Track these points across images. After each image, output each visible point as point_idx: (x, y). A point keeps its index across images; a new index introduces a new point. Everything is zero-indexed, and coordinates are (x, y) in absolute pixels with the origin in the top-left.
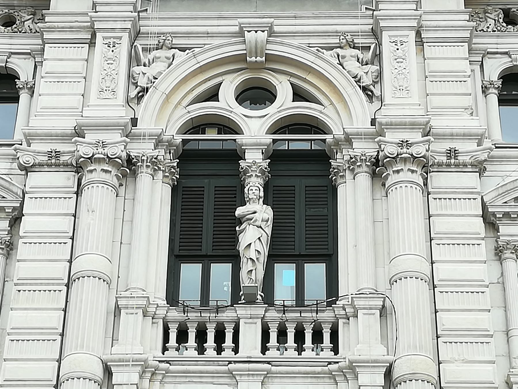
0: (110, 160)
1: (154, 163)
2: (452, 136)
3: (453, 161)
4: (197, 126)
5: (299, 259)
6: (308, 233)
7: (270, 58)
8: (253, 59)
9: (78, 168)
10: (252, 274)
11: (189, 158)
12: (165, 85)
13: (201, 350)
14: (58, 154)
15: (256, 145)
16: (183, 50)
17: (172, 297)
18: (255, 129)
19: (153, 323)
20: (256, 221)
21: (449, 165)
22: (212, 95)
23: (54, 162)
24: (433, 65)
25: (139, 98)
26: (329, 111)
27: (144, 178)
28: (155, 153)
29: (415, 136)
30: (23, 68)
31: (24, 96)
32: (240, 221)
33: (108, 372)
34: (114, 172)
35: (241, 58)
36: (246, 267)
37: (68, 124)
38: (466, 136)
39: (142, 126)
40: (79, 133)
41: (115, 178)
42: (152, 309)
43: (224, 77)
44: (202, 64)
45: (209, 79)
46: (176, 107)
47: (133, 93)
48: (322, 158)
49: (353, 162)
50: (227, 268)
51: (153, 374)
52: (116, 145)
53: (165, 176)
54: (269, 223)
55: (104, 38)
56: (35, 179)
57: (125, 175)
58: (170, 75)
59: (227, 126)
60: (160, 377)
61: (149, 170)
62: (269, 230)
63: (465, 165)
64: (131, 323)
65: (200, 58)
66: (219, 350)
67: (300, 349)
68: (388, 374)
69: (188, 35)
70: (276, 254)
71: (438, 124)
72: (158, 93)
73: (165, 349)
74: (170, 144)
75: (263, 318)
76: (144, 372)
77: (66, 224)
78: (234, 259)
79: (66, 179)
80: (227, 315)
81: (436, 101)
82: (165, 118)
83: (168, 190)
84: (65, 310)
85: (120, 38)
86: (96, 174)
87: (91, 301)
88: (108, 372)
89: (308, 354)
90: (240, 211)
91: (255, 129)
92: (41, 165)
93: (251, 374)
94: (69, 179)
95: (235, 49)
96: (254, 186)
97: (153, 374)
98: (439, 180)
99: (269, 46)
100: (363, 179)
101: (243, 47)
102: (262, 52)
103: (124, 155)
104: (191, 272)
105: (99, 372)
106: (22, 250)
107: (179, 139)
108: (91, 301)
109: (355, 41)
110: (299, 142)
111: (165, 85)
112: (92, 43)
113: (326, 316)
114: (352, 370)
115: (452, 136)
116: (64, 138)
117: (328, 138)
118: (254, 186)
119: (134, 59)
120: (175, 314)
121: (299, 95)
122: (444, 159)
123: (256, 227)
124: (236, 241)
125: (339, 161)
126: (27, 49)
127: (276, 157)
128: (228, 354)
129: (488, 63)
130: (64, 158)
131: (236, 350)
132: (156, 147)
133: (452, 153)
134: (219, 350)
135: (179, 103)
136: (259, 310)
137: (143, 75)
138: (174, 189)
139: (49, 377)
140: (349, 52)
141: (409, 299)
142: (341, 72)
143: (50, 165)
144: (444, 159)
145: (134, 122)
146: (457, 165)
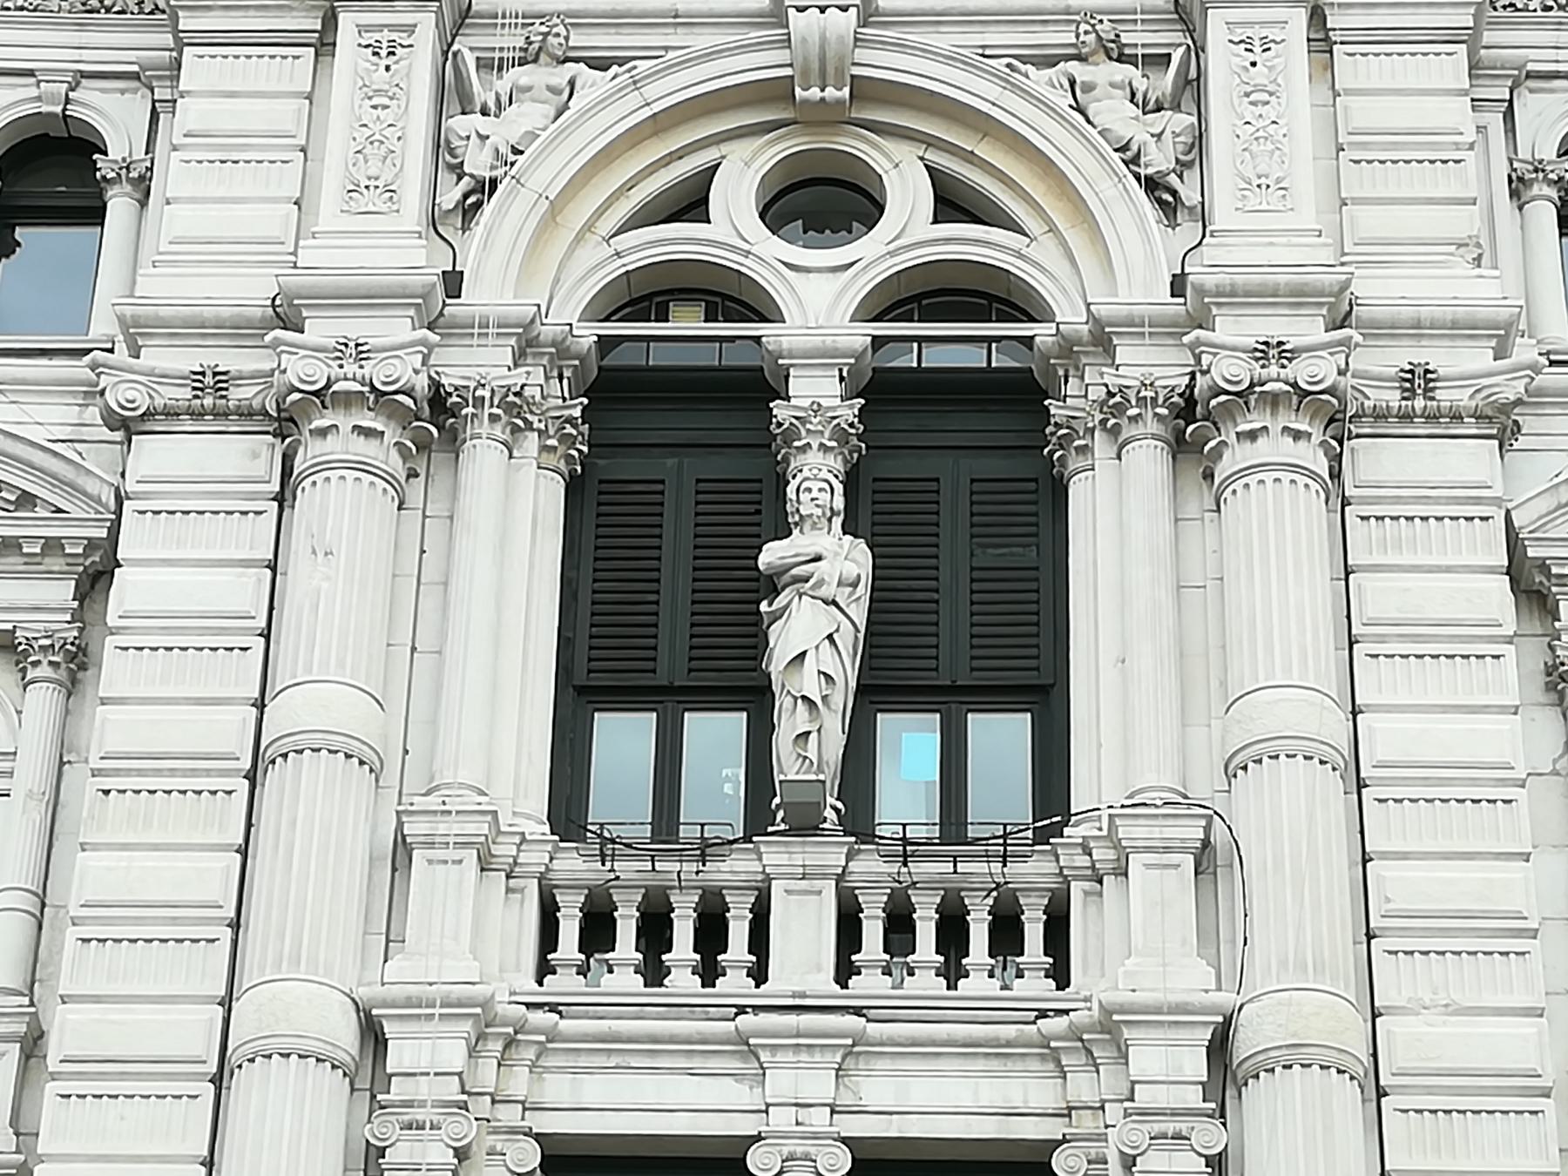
0: (380, 398)
1: (514, 406)
2: (1418, 329)
3: (1419, 403)
4: (644, 295)
5: (954, 700)
6: (978, 620)
7: (864, 91)
8: (815, 93)
9: (284, 422)
10: (809, 745)
11: (617, 393)
12: (547, 172)
13: (654, 972)
14: (223, 380)
15: (820, 356)
16: (600, 65)
17: (568, 813)
18: (819, 305)
19: (508, 890)
20: (820, 583)
21: (1406, 417)
22: (690, 203)
23: (210, 404)
24: (1360, 113)
25: (468, 211)
26: (1045, 250)
27: (483, 452)
28: (517, 378)
29: (1306, 329)
30: (116, 120)
31: (119, 205)
32: (771, 585)
33: (373, 1036)
34: (392, 434)
35: (777, 91)
36: (789, 722)
37: (252, 290)
38: (1461, 328)
39: (477, 298)
40: (285, 316)
41: (394, 453)
42: (505, 850)
43: (725, 148)
44: (657, 107)
45: (678, 155)
46: (579, 239)
47: (451, 195)
48: (1019, 396)
49: (1115, 405)
50: (731, 726)
51: (510, 1042)
52: (398, 355)
53: (544, 449)
54: (861, 589)
55: (362, 29)
56: (154, 455)
57: (424, 446)
58: (561, 140)
59: (733, 298)
60: (530, 1054)
61: (497, 431)
62: (860, 614)
63: (1457, 417)
64: (444, 890)
65: (651, 91)
66: (709, 972)
67: (953, 972)
68: (1220, 1046)
69: (615, 19)
70: (880, 689)
71: (1375, 290)
72: (525, 198)
73: (544, 969)
74: (561, 351)
75: (840, 878)
76: (481, 1037)
77: (248, 592)
78: (754, 697)
79: (246, 457)
80: (734, 868)
81: (1369, 222)
82: (546, 273)
83: (554, 491)
84: (244, 851)
85: (410, 29)
86: (336, 441)
87: (323, 823)
88: (373, 1036)
89: (977, 984)
90: (771, 555)
91: (819, 305)
92: (171, 413)
93: (803, 1044)
94: (255, 455)
95: (761, 64)
96: (816, 478)
97: (510, 1042)
98: (1378, 462)
99: (861, 55)
100: (1148, 457)
101: (783, 56)
102: (840, 72)
103: (421, 383)
104: (623, 740)
105: (346, 1037)
106: (115, 669)
107: (587, 335)
108: (323, 823)
109: (1125, 39)
110: (953, 346)
111: (547, 172)
112: (324, 44)
113: (1032, 871)
114: (1110, 1033)
115: (1418, 329)
116: (241, 330)
117: (1042, 333)
118: (816, 478)
119: (452, 93)
120: (575, 865)
121: (952, 202)
122: (1392, 398)
123: (820, 599)
124: (759, 644)
125: (1073, 402)
126: (127, 61)
127: (883, 392)
128: (734, 983)
129: (1528, 106)
130: (240, 394)
131: (759, 974)
132: (519, 358)
133: (1417, 380)
134: (709, 972)
135: (589, 226)
136: (830, 853)
137: (479, 141)
138: (575, 488)
139: (197, 1051)
140: (1106, 72)
141: (1287, 819)
142: (1076, 134)
143: (197, 415)
144: (1392, 398)
145: (453, 283)
146: (1432, 417)
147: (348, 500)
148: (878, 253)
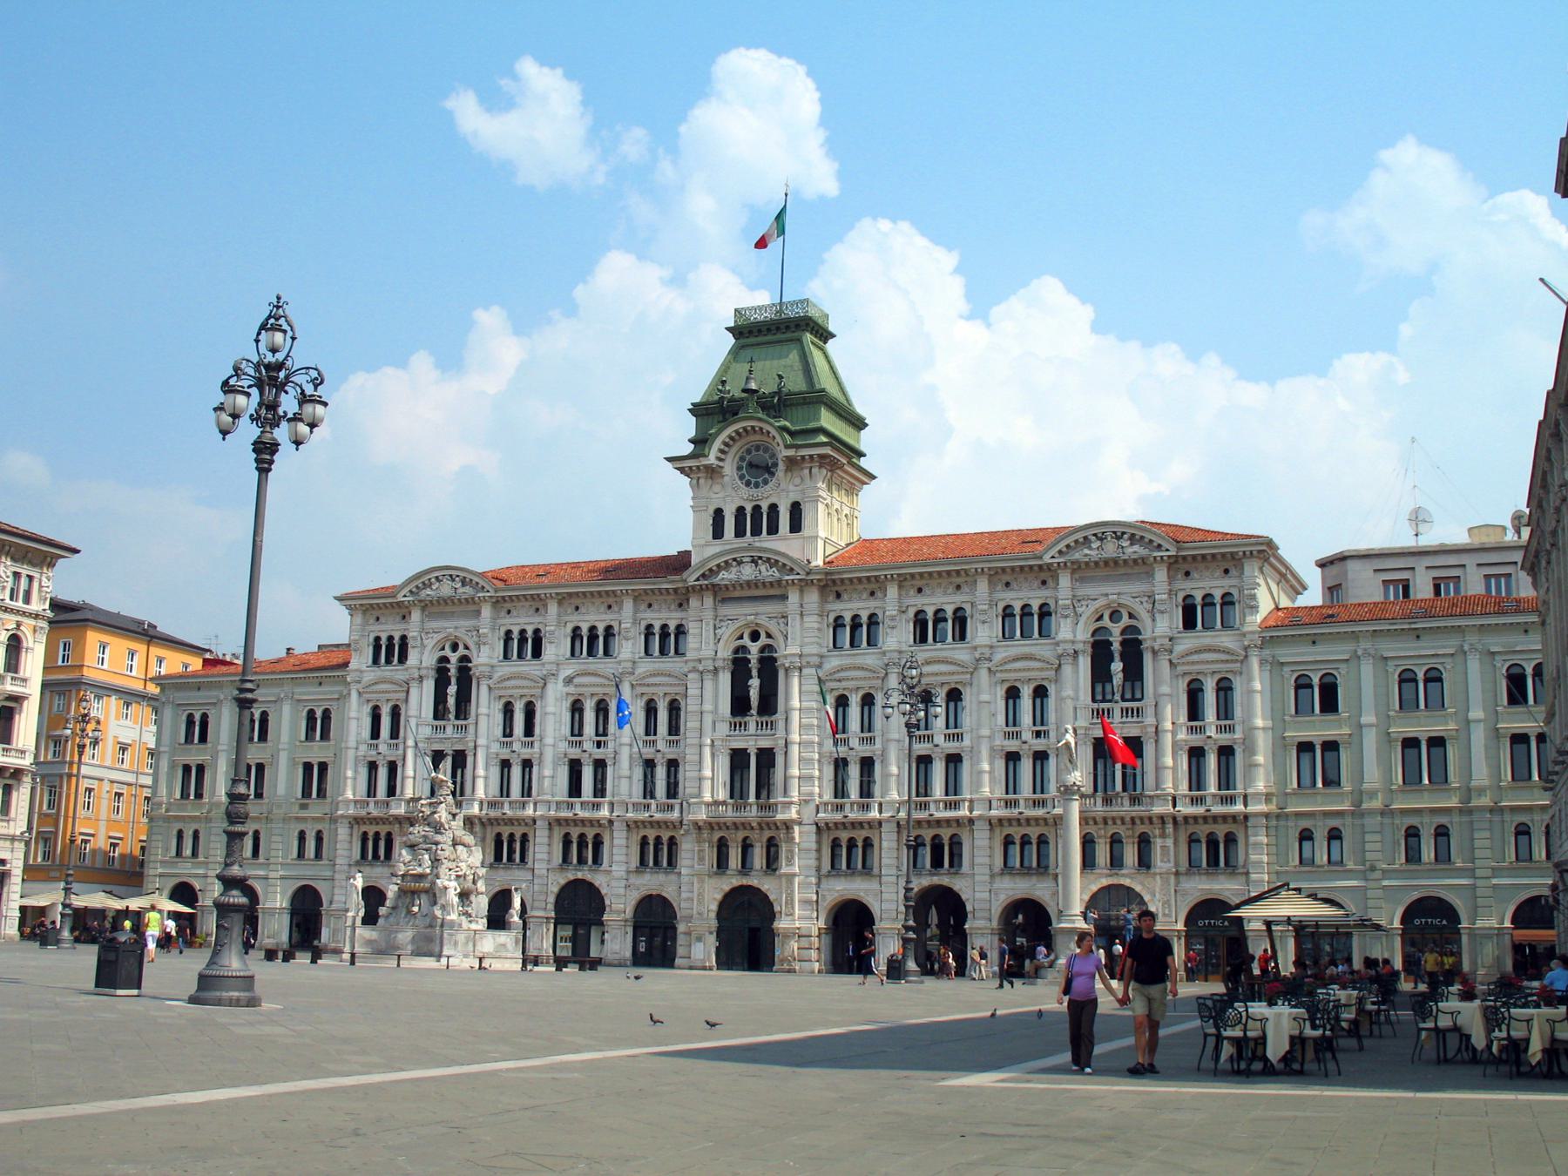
4: (737, 651)
11: (735, 661)
22: (741, 637)
23: (695, 670)
27: (721, 674)
40: (700, 661)
56: (690, 676)
58: (728, 631)
71: (806, 650)
91: (754, 649)
96: (754, 673)
98: (805, 671)
108: (708, 720)
111: (725, 637)
118: (754, 673)
127: (761, 660)
147: (708, 678)
148: (759, 643)
